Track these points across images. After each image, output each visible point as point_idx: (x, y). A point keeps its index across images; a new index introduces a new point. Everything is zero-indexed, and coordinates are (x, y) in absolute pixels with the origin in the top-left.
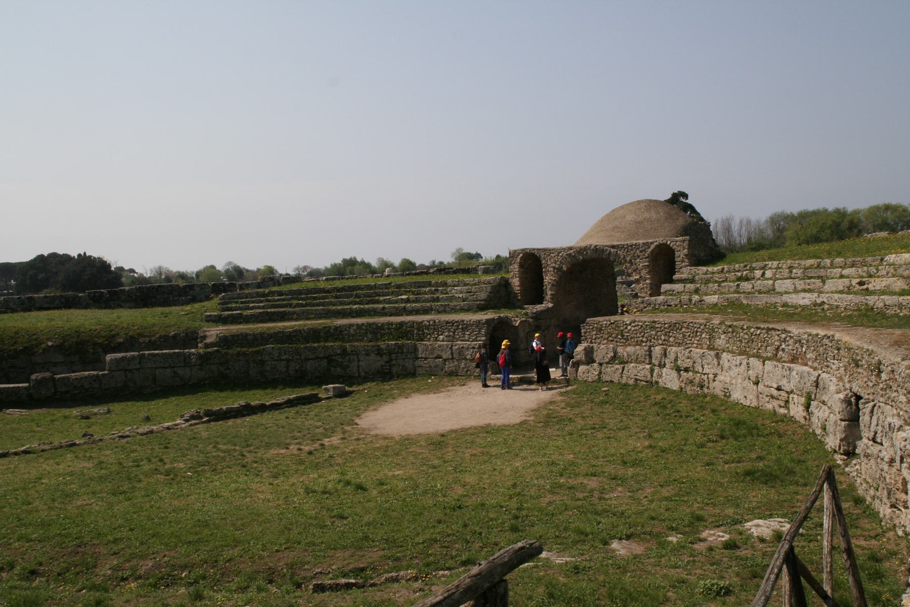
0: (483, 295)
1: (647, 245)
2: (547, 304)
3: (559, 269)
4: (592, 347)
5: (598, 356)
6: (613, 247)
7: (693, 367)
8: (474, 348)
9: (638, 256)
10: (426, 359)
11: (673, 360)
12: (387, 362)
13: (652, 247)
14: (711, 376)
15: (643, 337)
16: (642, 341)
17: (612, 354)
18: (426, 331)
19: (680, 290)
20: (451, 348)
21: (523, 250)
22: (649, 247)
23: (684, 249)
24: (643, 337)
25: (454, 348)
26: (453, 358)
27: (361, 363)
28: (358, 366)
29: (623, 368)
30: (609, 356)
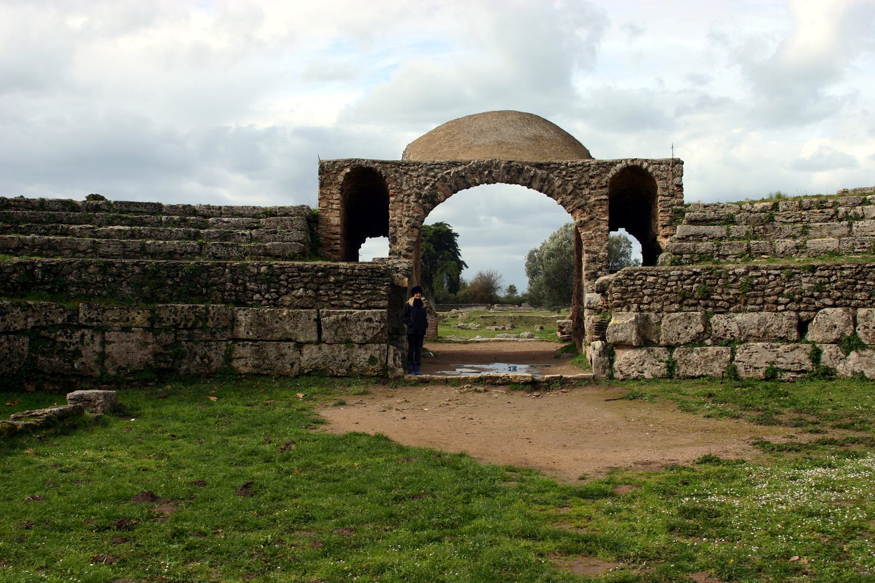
4: (647, 318)
6: (539, 166)
8: (370, 320)
13: (613, 171)
16: (777, 303)
19: (719, 234)
22: (608, 171)
25: (326, 320)
26: (320, 341)
27: (109, 348)
29: (733, 353)
30: (693, 332)
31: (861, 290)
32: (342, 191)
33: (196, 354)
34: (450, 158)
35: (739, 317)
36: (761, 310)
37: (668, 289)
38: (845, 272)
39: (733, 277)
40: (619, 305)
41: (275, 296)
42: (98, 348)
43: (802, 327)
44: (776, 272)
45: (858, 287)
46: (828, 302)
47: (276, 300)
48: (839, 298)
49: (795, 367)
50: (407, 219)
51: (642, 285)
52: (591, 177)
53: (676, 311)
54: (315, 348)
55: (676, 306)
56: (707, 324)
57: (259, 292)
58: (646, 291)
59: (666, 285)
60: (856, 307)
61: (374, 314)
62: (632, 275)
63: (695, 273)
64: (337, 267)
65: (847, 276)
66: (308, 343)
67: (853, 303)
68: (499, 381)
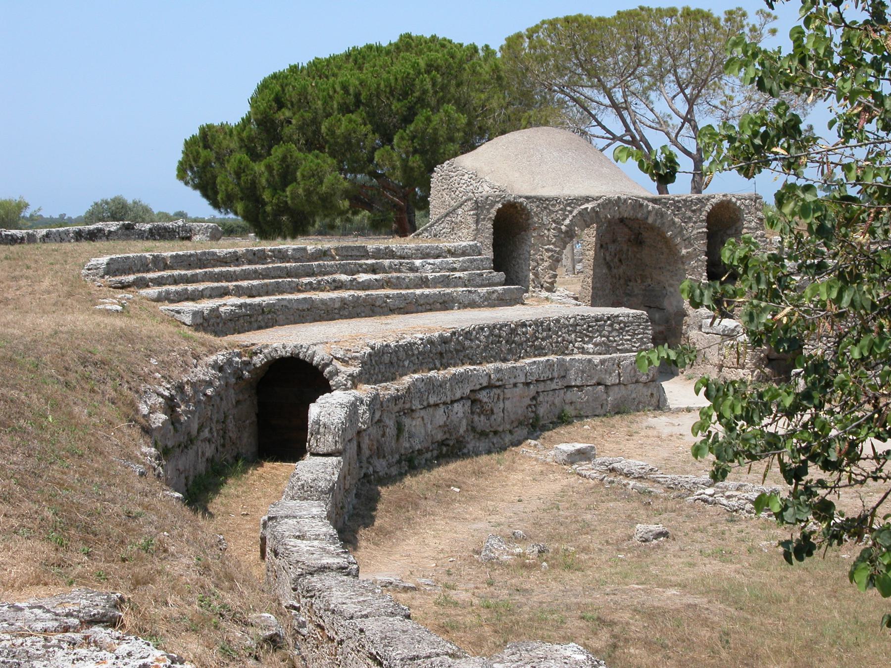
9: (690, 218)
13: (708, 208)
42: (501, 405)
50: (550, 254)
52: (694, 211)
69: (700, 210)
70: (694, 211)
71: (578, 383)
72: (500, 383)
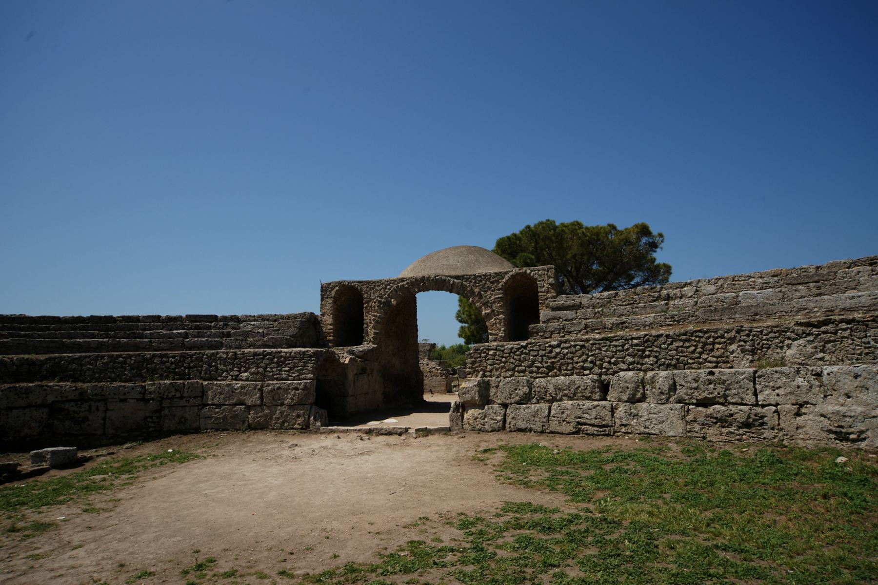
0: (292, 331)
1: (500, 275)
2: (365, 347)
3: (388, 303)
5: (498, 395)
6: (457, 277)
7: (725, 396)
8: (297, 389)
9: (489, 288)
10: (219, 406)
11: (665, 389)
12: (156, 411)
13: (506, 278)
14: (787, 407)
15: (585, 361)
17: (526, 389)
18: (221, 367)
19: (570, 317)
20: (261, 390)
21: (340, 283)
22: (503, 278)
23: (549, 277)
24: (585, 361)
25: (266, 389)
28: (104, 419)
30: (521, 393)
31: (649, 356)
32: (335, 302)
33: (175, 415)
34: (400, 276)
35: (554, 380)
36: (572, 374)
37: (504, 360)
38: (635, 341)
39: (549, 349)
40: (470, 373)
41: (237, 373)
43: (605, 388)
44: (581, 343)
45: (647, 353)
46: (624, 367)
47: (237, 376)
48: (633, 363)
49: (597, 422)
51: (485, 357)
52: (492, 283)
53: (511, 376)
54: (259, 409)
55: (510, 373)
56: (530, 385)
57: (227, 371)
58: (489, 362)
59: (503, 357)
60: (645, 371)
61: (300, 384)
62: (478, 349)
63: (522, 347)
64: (281, 352)
65: (637, 345)
66: (254, 406)
67: (644, 367)
68: (383, 431)
69: (498, 282)
70: (492, 283)
71: (216, 401)
72: (100, 398)
